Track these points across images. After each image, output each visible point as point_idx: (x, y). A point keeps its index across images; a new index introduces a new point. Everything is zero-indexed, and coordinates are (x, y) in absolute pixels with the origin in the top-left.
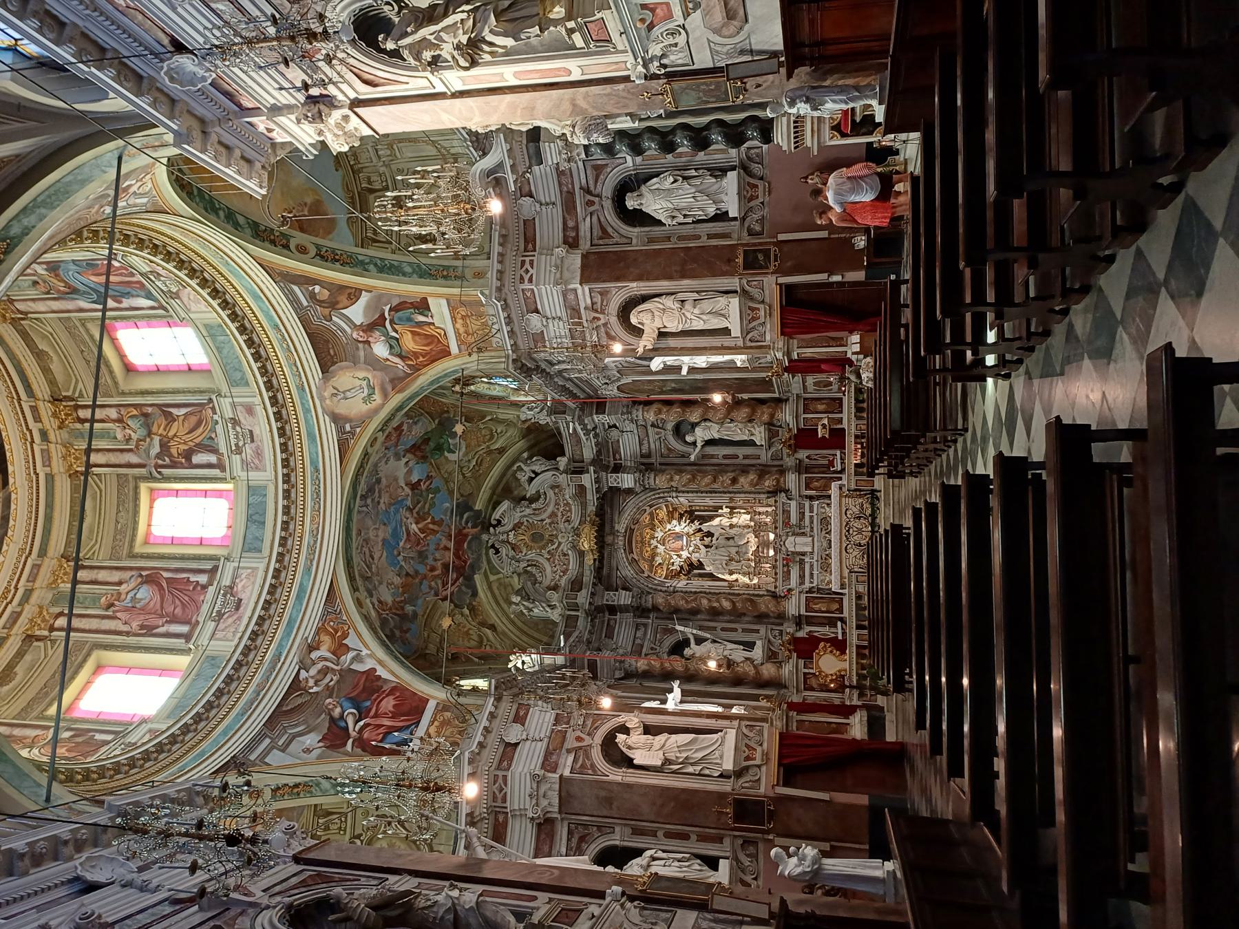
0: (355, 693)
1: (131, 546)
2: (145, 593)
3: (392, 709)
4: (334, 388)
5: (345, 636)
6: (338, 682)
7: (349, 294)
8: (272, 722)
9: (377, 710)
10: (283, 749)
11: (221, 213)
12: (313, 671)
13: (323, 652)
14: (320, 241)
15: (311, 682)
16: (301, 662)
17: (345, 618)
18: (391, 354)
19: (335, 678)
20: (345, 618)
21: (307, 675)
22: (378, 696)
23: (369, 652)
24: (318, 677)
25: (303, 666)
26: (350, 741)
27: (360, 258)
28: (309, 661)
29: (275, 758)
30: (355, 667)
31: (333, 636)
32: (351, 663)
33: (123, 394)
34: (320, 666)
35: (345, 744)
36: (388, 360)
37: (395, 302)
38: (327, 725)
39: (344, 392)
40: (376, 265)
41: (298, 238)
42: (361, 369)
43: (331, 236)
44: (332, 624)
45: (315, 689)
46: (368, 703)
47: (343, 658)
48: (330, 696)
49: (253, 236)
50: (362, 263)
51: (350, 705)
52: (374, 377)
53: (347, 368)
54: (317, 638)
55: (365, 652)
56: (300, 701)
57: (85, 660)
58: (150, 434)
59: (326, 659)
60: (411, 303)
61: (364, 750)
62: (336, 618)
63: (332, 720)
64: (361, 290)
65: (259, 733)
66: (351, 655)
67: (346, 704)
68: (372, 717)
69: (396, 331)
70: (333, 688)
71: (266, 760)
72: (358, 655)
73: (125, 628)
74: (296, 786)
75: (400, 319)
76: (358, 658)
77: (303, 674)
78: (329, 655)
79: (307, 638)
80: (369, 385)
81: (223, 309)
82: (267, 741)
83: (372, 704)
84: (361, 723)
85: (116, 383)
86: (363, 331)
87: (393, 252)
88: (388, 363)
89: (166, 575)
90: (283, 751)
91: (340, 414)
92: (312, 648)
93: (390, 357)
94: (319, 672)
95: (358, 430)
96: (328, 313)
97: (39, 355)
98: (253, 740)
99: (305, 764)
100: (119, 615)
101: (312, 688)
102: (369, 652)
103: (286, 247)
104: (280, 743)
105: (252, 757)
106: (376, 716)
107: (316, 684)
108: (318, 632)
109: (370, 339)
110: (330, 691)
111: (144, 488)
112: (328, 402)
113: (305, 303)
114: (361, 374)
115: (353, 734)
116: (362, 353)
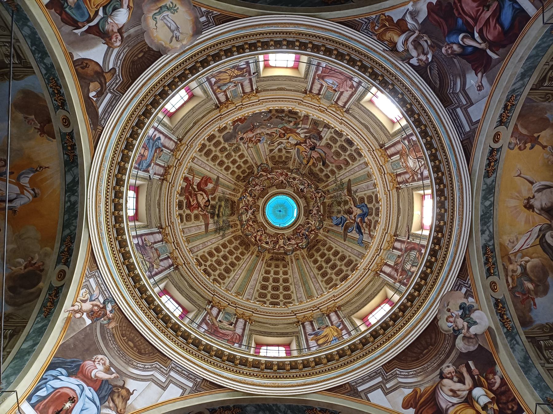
0: (445, 27)
1: (300, 78)
2: (330, 81)
3: (475, 5)
4: (171, 41)
5: (390, 19)
6: (430, 37)
7: (83, 68)
8: (446, 101)
9: (470, 17)
10: (471, 103)
11: (73, 199)
12: (414, 53)
13: (400, 40)
14: (50, 107)
15: (423, 58)
16: (403, 61)
17: (374, 16)
18: (122, 6)
19: (425, 38)
20: (374, 16)
21: (415, 59)
22: (457, 10)
23: (411, 3)
24: (420, 51)
25: (407, 59)
26: (488, 51)
27: (44, 72)
28: (405, 54)
29: (475, 112)
30: (420, 21)
31: (388, 29)
32: (416, 21)
33: (208, 96)
34: (411, 47)
35: (490, 57)
36: (128, 6)
37: (67, 28)
38: (464, 61)
39: (173, 31)
40: (42, 58)
41: (57, 125)
42: (147, 25)
43: (40, 95)
44: (377, 28)
45: (430, 57)
46: (460, 21)
47: (409, 26)
48: (441, 48)
49: (77, 166)
50: (47, 69)
51: (455, 36)
52: (150, 11)
53: (150, 37)
54: (386, 42)
55: (410, 7)
56: (435, 72)
57: (365, 108)
58: (230, 82)
59: (406, 40)
60: (60, 14)
61: (504, 46)
62: (372, 23)
63: (462, 55)
64: (74, 62)
65: (450, 114)
66: (409, 19)
67: (453, 39)
68: (476, 24)
69: (97, 13)
70: (433, 42)
71: (474, 121)
72: (411, 13)
73: (350, 93)
74: (506, 107)
75: (83, 15)
76: (414, 14)
77: (414, 61)
78: (403, 37)
79: (384, 49)
80: (159, 13)
81: (138, 135)
82: (459, 110)
83: (462, 18)
84: (476, 35)
85: (203, 101)
86: (111, 39)
87: (18, 41)
88: (131, 5)
89: (319, 72)
90: (472, 104)
91: (193, 27)
92: (393, 49)
93: (125, 6)
94: (416, 48)
95: (203, 9)
96: (109, 74)
97: (195, 123)
98: (454, 121)
99: (491, 96)
100: (341, 90)
101: (427, 59)
102: (411, 3)
103: (71, 135)
104: (465, 103)
105: (468, 129)
106: (476, 20)
107: (426, 54)
108: (380, 39)
109: (116, 30)
110: (435, 47)
111: (263, 74)
112: (184, 43)
113: (109, 96)
114: (152, 23)
115: (483, 46)
116: (132, 31)
